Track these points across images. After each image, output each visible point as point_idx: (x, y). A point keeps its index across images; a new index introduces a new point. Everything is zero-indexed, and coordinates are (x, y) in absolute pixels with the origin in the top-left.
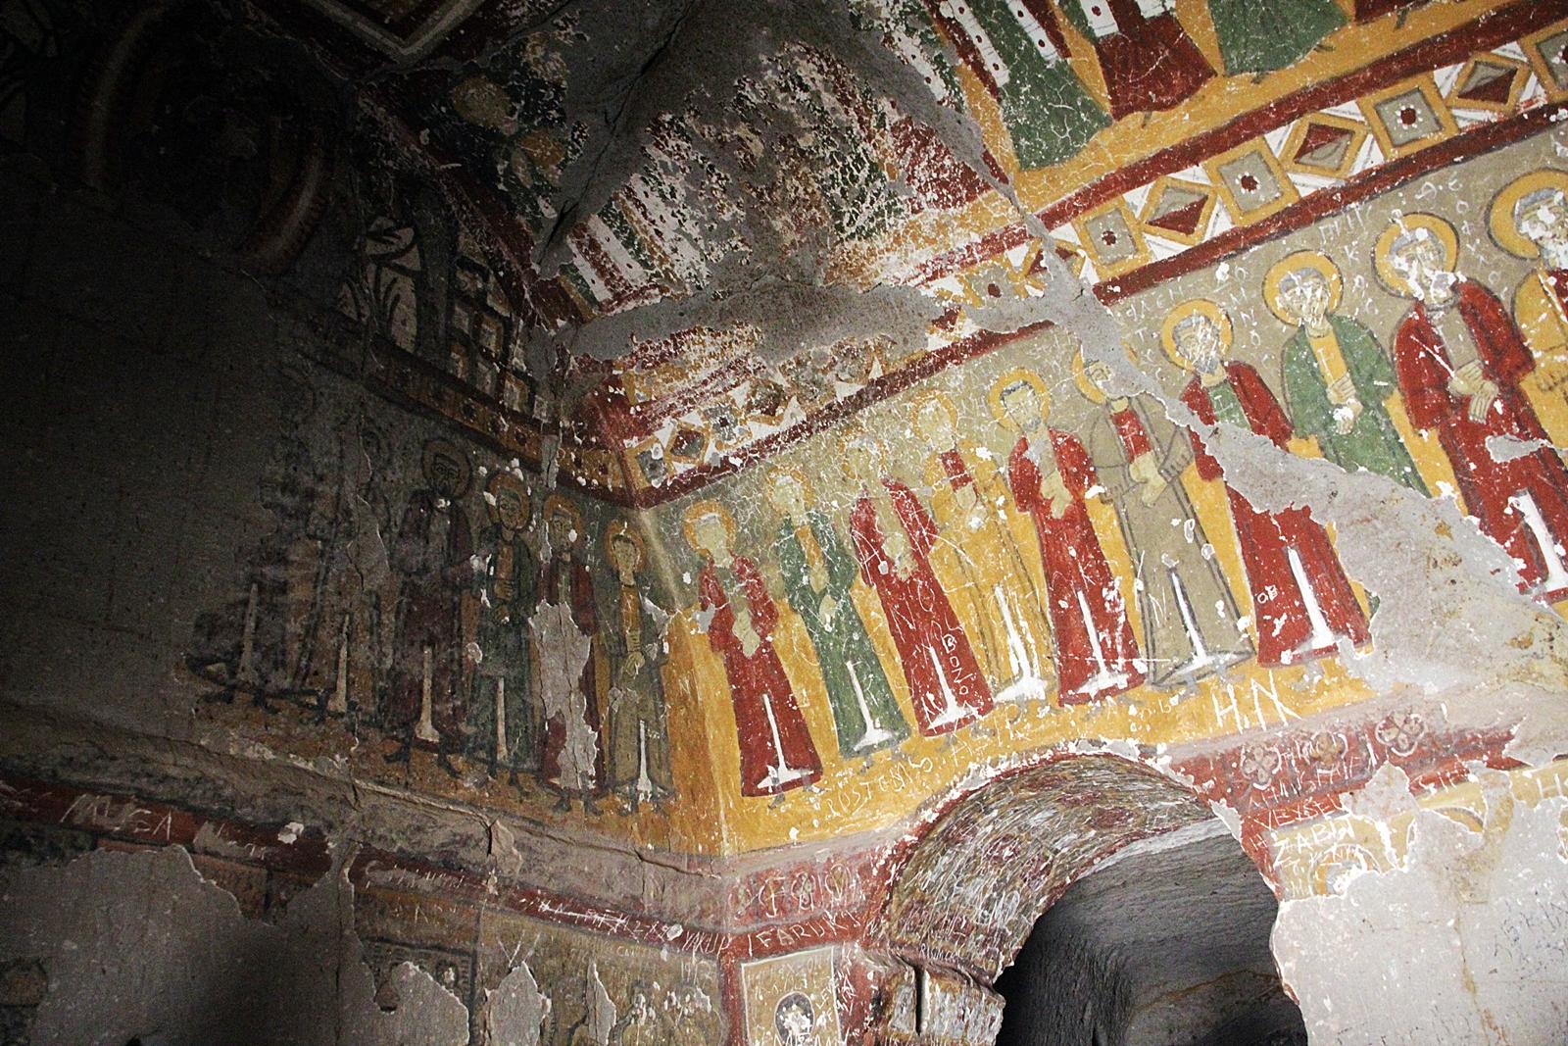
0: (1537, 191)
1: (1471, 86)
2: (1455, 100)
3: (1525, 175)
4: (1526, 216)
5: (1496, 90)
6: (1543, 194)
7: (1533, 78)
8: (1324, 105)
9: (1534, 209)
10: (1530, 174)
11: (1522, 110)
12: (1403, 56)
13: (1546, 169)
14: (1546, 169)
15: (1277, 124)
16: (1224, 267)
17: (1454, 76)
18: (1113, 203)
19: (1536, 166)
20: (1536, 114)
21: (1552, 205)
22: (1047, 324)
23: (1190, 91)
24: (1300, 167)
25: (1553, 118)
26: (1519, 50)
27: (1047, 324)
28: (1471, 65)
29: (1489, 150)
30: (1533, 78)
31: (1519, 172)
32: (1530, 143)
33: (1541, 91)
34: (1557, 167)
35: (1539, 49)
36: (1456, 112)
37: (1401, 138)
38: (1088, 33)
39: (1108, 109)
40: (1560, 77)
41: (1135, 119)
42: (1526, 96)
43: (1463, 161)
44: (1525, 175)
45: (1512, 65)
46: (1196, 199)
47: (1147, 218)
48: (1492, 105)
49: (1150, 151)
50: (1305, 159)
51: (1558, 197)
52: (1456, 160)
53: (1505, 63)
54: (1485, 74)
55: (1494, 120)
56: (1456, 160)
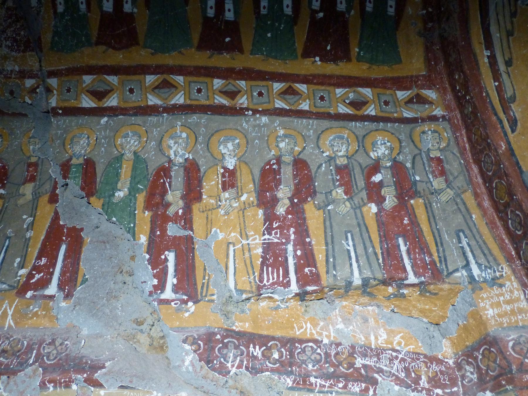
0: (231, 136)
1: (224, 90)
2: (217, 92)
3: (229, 129)
4: (223, 144)
5: (232, 95)
6: (232, 138)
7: (245, 97)
8: (172, 74)
9: (227, 142)
10: (231, 129)
11: (238, 106)
12: (206, 68)
13: (237, 130)
14: (237, 130)
15: (152, 74)
16: (106, 119)
17: (220, 84)
18: (77, 77)
19: (234, 127)
20: (242, 109)
21: (234, 143)
22: (25, 115)
23: (127, 47)
24: (153, 93)
25: (246, 113)
26: (245, 85)
27: (25, 115)
28: (228, 82)
29: (221, 114)
30: (245, 97)
31: (228, 127)
32: (236, 118)
33: (246, 102)
34: (241, 130)
35: (251, 88)
36: (216, 96)
37: (193, 97)
38: (101, 7)
39: (94, 40)
40: (254, 100)
41: (101, 48)
42: (241, 102)
43: (211, 114)
44: (229, 129)
45: (241, 89)
46: (109, 88)
47: (87, 88)
48: (229, 99)
49: (101, 63)
50: (156, 91)
51: (237, 141)
52: (208, 113)
53: (239, 87)
54: (230, 88)
55: (227, 105)
56: (208, 113)
